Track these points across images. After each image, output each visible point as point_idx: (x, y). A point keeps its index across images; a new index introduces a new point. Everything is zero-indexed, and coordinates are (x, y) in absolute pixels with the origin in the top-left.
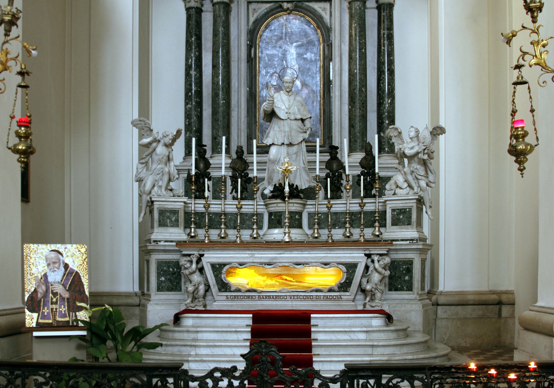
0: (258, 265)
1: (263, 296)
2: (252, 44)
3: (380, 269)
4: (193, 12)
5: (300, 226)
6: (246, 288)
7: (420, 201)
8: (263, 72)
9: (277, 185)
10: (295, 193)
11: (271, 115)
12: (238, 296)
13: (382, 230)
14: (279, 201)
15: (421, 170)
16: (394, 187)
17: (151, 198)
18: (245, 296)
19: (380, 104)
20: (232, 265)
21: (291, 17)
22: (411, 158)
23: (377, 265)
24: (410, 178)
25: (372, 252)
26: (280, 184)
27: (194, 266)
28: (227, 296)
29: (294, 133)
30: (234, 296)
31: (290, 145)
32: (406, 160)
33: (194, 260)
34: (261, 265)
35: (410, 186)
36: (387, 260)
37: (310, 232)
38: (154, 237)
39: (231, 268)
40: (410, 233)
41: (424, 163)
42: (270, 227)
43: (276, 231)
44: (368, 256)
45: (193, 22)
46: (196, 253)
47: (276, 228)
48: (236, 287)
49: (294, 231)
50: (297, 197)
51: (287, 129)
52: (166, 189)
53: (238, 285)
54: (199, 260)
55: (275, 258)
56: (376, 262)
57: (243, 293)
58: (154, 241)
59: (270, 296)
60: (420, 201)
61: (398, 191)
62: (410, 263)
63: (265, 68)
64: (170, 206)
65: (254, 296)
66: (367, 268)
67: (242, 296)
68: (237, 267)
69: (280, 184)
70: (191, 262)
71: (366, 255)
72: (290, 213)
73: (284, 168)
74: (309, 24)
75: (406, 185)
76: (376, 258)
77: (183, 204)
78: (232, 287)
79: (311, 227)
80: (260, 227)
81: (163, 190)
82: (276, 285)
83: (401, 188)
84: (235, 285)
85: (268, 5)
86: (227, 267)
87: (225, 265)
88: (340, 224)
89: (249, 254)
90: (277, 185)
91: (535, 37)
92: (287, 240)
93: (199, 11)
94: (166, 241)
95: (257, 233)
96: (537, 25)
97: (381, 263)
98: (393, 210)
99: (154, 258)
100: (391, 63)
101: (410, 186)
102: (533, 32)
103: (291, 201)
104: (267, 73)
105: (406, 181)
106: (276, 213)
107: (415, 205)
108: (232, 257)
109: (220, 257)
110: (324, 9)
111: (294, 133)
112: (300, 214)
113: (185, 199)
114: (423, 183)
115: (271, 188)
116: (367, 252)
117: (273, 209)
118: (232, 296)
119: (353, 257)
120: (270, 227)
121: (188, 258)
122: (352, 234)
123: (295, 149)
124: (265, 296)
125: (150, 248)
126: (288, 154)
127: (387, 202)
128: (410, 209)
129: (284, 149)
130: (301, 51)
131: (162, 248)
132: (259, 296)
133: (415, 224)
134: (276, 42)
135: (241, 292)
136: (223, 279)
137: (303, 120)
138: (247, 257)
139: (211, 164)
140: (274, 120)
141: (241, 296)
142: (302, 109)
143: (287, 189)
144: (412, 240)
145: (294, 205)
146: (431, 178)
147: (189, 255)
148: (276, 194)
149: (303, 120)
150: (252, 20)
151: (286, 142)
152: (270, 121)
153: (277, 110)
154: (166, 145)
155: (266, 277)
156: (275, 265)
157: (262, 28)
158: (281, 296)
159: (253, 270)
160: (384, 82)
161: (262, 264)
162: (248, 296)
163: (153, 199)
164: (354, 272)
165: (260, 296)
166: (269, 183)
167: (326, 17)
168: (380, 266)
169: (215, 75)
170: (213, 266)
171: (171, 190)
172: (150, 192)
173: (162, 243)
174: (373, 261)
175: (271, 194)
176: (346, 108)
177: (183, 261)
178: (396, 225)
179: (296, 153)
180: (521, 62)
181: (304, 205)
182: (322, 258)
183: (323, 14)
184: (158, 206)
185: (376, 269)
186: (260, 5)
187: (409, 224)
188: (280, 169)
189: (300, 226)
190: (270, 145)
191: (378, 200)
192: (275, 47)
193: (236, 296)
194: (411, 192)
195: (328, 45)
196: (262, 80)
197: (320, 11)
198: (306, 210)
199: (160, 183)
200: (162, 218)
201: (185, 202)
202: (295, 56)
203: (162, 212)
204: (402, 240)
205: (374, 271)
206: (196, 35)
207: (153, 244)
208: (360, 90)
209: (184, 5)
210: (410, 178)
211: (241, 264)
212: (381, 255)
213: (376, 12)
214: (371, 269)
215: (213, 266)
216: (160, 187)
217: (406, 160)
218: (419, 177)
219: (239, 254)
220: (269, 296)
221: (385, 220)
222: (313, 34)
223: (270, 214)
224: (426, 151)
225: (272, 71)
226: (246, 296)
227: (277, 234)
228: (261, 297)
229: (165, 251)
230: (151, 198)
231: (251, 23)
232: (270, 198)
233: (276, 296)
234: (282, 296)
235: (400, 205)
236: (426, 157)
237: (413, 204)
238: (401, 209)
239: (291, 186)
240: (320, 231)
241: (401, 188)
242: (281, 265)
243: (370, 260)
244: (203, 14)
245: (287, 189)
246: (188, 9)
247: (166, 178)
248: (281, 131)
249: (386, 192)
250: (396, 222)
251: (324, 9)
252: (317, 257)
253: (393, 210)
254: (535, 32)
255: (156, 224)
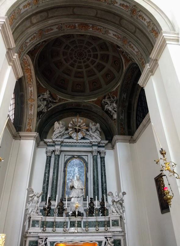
2: (65, 167)
3: (110, 243)
4: (49, 157)
5: (81, 227)
7: (121, 217)
8: (68, 175)
9: (74, 211)
10: (80, 214)
11: (72, 187)
13: (108, 228)
14: (74, 217)
15: (120, 206)
16: (112, 212)
17: (30, 216)
19: (102, 185)
20: (57, 242)
21: (77, 159)
22: (117, 202)
23: (109, 242)
24: (117, 209)
25: (107, 237)
26: (75, 211)
27: (43, 243)
29: (79, 193)
31: (78, 197)
32: (115, 203)
33: (44, 240)
35: (117, 212)
36: (112, 240)
37: (84, 229)
38: (29, 231)
39: (57, 243)
40: (119, 229)
41: (121, 204)
42: (70, 227)
43: (73, 228)
44: (106, 238)
45: (48, 160)
46: (45, 238)
47: (72, 227)
49: (79, 228)
50: (80, 216)
51: (77, 192)
52: (36, 213)
54: (46, 240)
55: (73, 239)
56: (109, 240)
58: (29, 233)
60: (121, 217)
61: (113, 213)
62: (120, 240)
63: (68, 174)
64: (36, 219)
66: (105, 243)
68: (59, 243)
69: (75, 211)
70: (43, 241)
71: (105, 238)
72: (78, 221)
73: (76, 205)
74: (81, 161)
75: (116, 212)
76: (109, 239)
77: (41, 218)
79: (85, 226)
80: (67, 227)
81: (35, 213)
83: (114, 213)
85: (70, 156)
86: (56, 243)
87: (55, 242)
88: (94, 226)
90: (74, 211)
91: (165, 162)
92: (76, 232)
93: (50, 157)
94: (33, 233)
95: (66, 229)
96: (165, 158)
97: (110, 241)
98: (112, 221)
99: (29, 239)
100: (105, 173)
101: (117, 212)
102: (164, 160)
103: (78, 217)
104: (69, 175)
105: (116, 210)
106: (73, 222)
107: (119, 219)
109: (53, 239)
110: (86, 158)
111: (79, 193)
112: (81, 222)
113: (42, 216)
114: (121, 211)
115: (71, 213)
116: (106, 237)
117: (72, 220)
119: (101, 239)
120: (70, 227)
121: (41, 240)
122: (98, 229)
123: (79, 199)
125: (27, 235)
126: (77, 201)
127: (110, 218)
128: (118, 220)
129: (76, 199)
130: (79, 169)
131: (32, 236)
133: (120, 226)
134: (72, 166)
137: (82, 189)
138: (63, 239)
139: (51, 204)
140: (73, 189)
142: (82, 185)
143: (77, 213)
144: (120, 232)
145: (78, 219)
146: (123, 209)
147: (42, 238)
148: (73, 214)
149: (82, 189)
150: (66, 160)
151: (77, 196)
152: (72, 189)
153: (74, 186)
154: (38, 197)
157: (68, 162)
160: (103, 179)
163: (31, 216)
164: (101, 244)
166: (71, 211)
167: (86, 160)
168: (110, 242)
169: (53, 176)
170: (50, 242)
171: (37, 213)
172: (30, 214)
173: (32, 233)
174: (107, 240)
175: (71, 215)
176: (92, 187)
177: (40, 241)
178: (114, 226)
179: (80, 200)
180: (162, 169)
181: (82, 218)
182: (90, 239)
183: (85, 159)
184: (32, 219)
185: (109, 243)
186: (68, 156)
187: (118, 226)
188: (75, 206)
189: (81, 227)
190: (72, 197)
191: (106, 217)
192: (72, 168)
194: (118, 214)
195: (87, 168)
196: (67, 177)
197: (84, 158)
198: (83, 221)
199: (34, 210)
200: (33, 224)
201: (42, 218)
202: (77, 170)
203: (33, 221)
204: (116, 232)
205: (108, 244)
206: (49, 164)
207: (29, 234)
208: (97, 181)
209: (46, 155)
210: (117, 209)
211: (61, 242)
212: (110, 238)
213: (100, 159)
214: (107, 243)
215: (50, 242)
216: (34, 212)
217: (115, 203)
218: (120, 209)
221: (110, 224)
222: (83, 165)
223: (71, 222)
224: (122, 200)
225: (70, 175)
227: (73, 229)
229: (33, 237)
230: (30, 216)
231: (65, 161)
232: (71, 216)
235: (114, 219)
236: (122, 202)
237: (119, 218)
238: (115, 220)
239: (78, 212)
240: (88, 228)
241: (114, 213)
243: (106, 240)
244: (52, 158)
245: (77, 213)
246: (47, 156)
247: (36, 209)
248: (75, 193)
249: (109, 214)
250: (113, 225)
251: (86, 158)
252: (88, 239)
253: (112, 221)
254: (165, 160)
255: (31, 226)
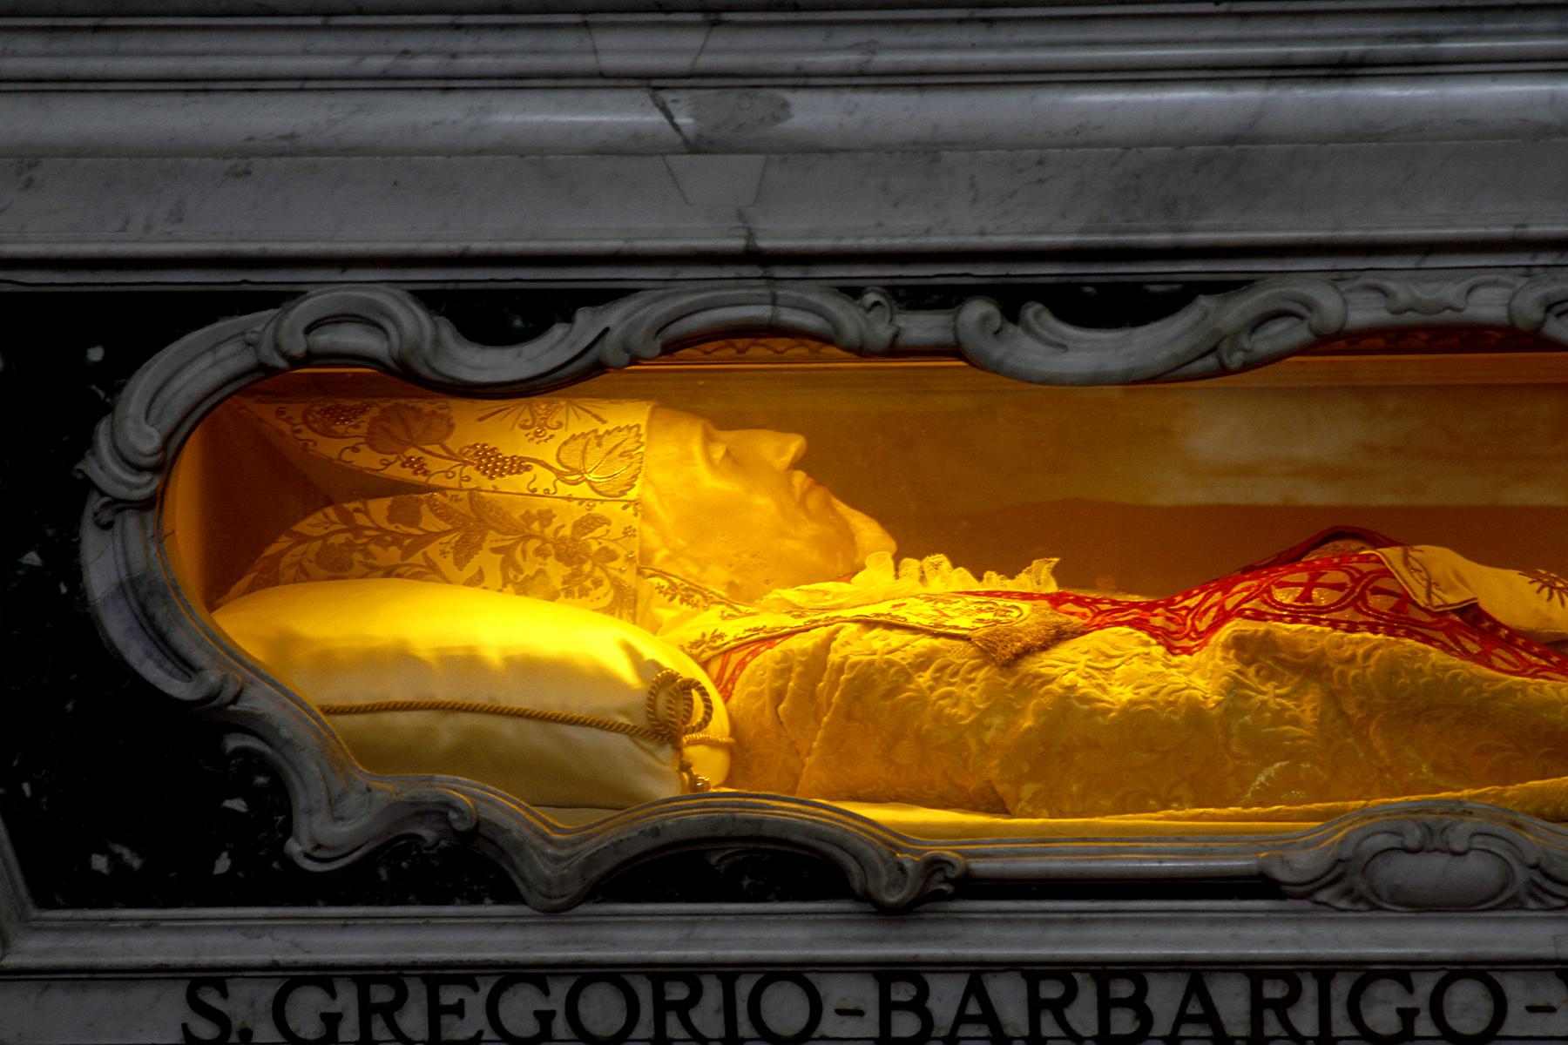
0: (849, 319)
1: (977, 974)
6: (622, 799)
12: (437, 976)
18: (586, 975)
28: (217, 978)
30: (364, 976)
34: (922, 327)
48: (389, 788)
53: (465, 757)
57: (557, 911)
59: (1138, 971)
65: (797, 974)
67: (537, 975)
78: (307, 796)
82: (1265, 749)
84: (377, 756)
89: (651, 82)
108: (289, 148)
118: (323, 977)
124: (1032, 972)
132: (886, 973)
135: (506, 892)
136: (118, 627)
141: (511, 975)
155: (1040, 576)
156: (1235, 311)
158: (1367, 973)
159: (794, 445)
161: (948, 298)
162: (660, 974)
165: (914, 972)
193: (394, 975)
219: (447, 83)
220: (1103, 972)
226: (614, 975)
228: (945, 998)
233: (1255, 972)
234: (1401, 972)
242: (1365, 312)
